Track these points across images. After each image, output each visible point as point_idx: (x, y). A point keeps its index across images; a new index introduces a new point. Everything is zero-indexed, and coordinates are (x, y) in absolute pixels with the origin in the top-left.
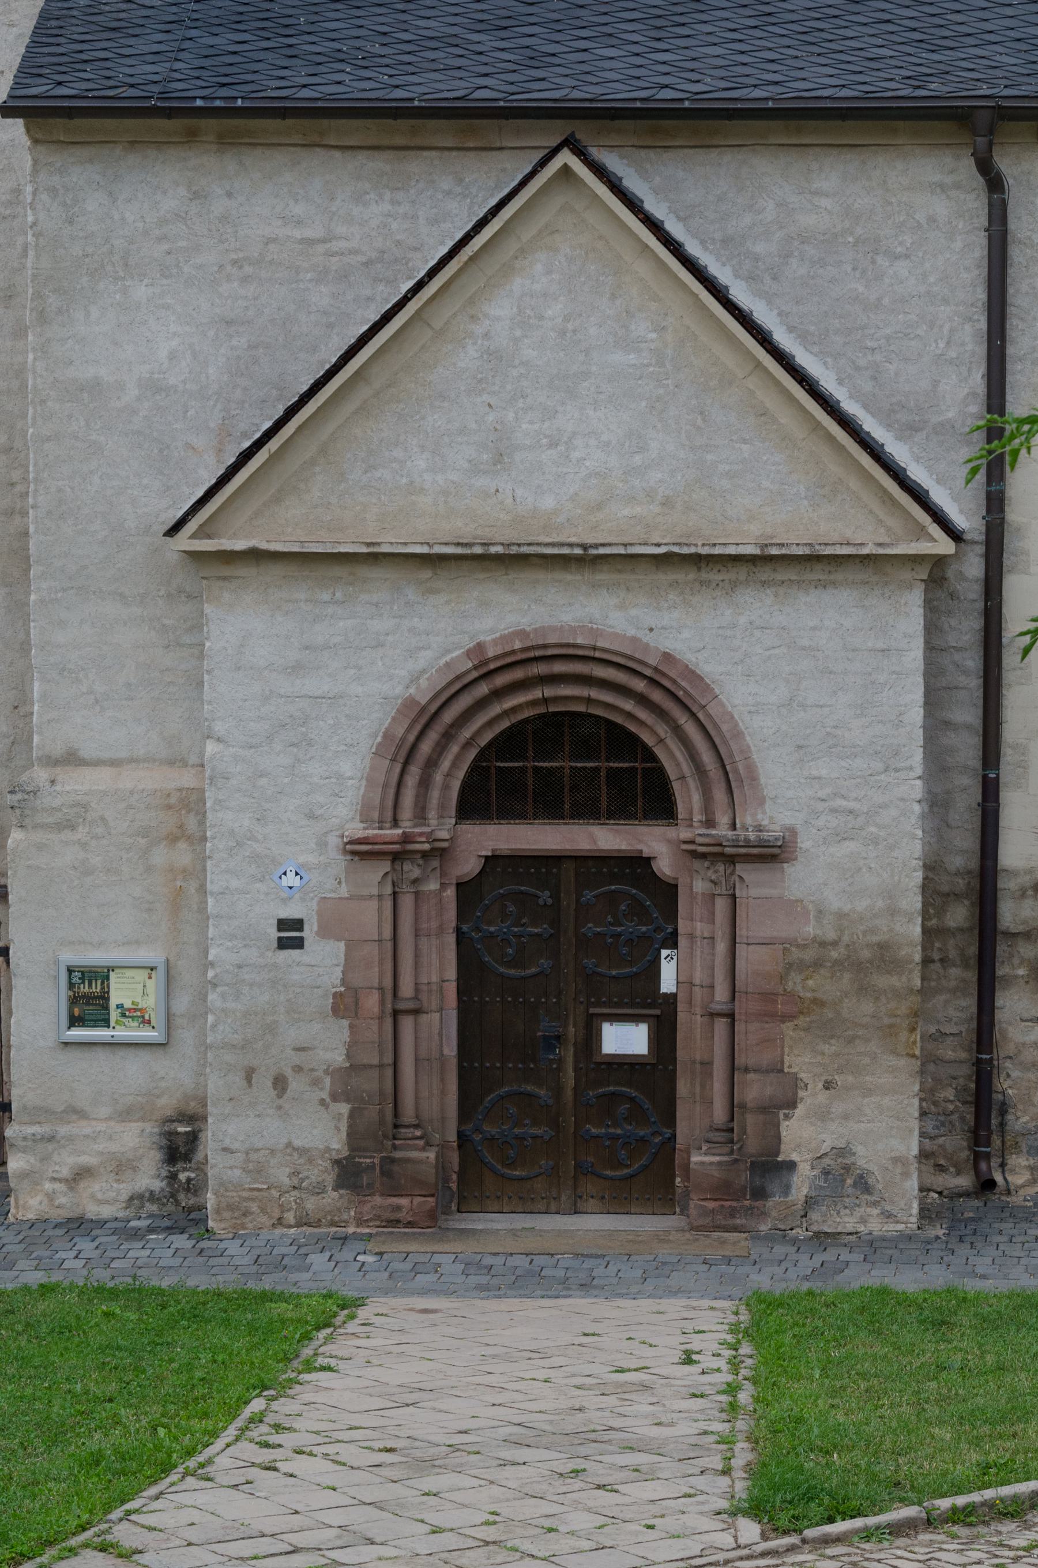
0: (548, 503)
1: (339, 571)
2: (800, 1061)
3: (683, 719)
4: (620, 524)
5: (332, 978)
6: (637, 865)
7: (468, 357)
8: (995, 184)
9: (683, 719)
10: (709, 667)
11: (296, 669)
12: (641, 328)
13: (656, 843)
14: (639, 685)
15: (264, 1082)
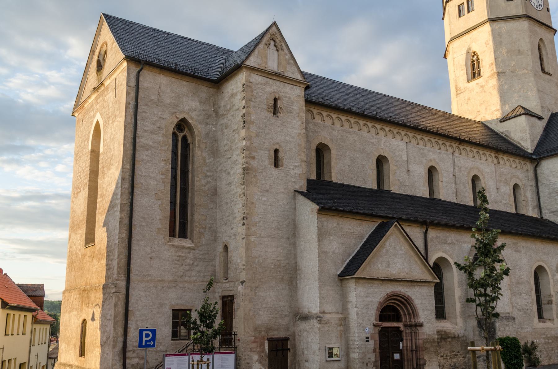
0: (394, 272)
1: (372, 281)
2: (426, 358)
3: (408, 306)
4: (402, 276)
5: (372, 347)
6: (398, 328)
7: (384, 250)
8: (426, 233)
9: (408, 306)
10: (413, 298)
11: (367, 297)
12: (403, 248)
13: (401, 325)
14: (403, 300)
15: (365, 364)
